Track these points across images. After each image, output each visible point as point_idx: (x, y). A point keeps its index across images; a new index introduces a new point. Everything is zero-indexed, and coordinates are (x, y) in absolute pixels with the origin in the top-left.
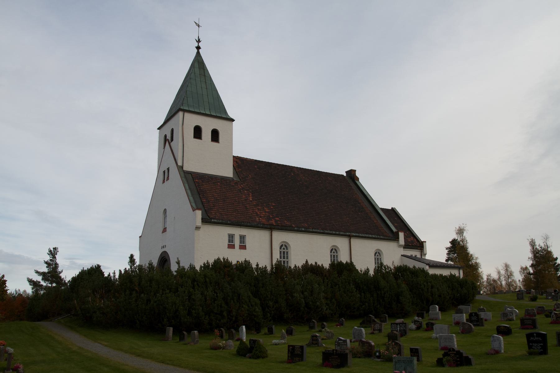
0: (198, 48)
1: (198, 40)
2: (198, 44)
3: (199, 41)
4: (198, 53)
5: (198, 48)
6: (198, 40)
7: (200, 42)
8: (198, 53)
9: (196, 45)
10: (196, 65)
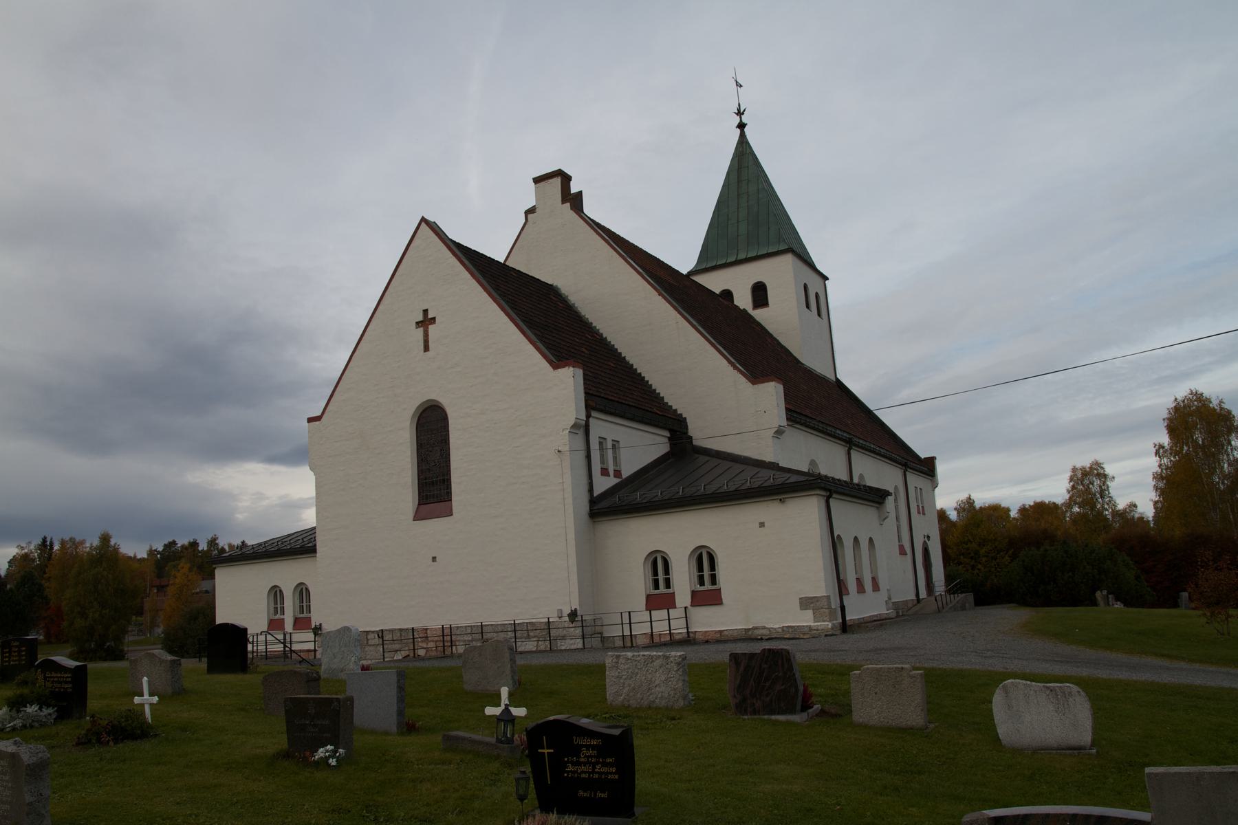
0: (742, 126)
1: (737, 112)
2: (741, 118)
3: (740, 113)
4: (743, 135)
5: (742, 126)
8: (743, 135)
9: (737, 120)
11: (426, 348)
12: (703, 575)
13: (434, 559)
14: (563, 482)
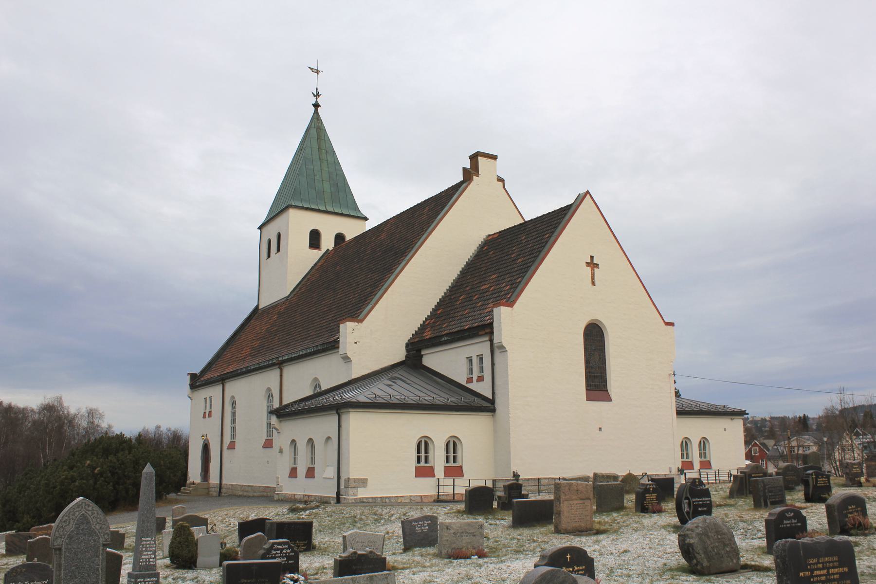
0: (316, 106)
1: (315, 94)
2: (317, 99)
3: (317, 95)
4: (316, 112)
5: (316, 106)
6: (315, 94)
7: (319, 96)
8: (316, 112)
9: (314, 101)
10: (314, 132)
11: (593, 283)
12: (425, 454)
13: (600, 429)
14: (671, 393)
